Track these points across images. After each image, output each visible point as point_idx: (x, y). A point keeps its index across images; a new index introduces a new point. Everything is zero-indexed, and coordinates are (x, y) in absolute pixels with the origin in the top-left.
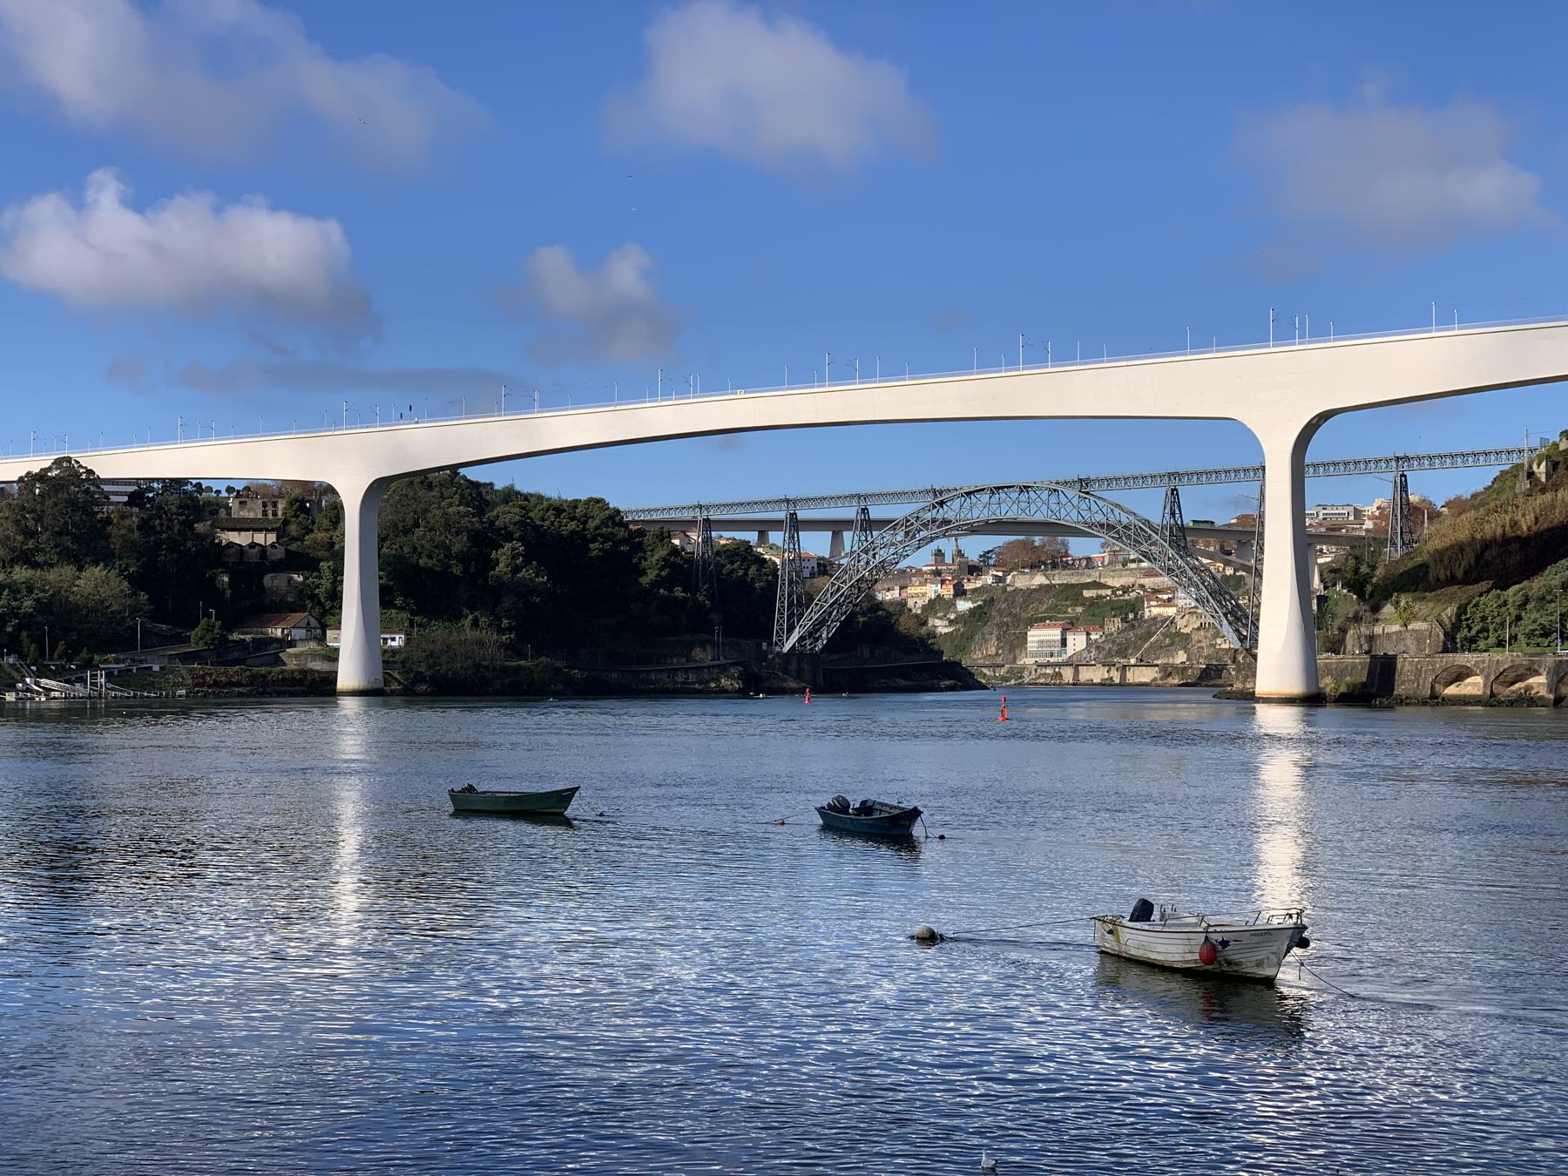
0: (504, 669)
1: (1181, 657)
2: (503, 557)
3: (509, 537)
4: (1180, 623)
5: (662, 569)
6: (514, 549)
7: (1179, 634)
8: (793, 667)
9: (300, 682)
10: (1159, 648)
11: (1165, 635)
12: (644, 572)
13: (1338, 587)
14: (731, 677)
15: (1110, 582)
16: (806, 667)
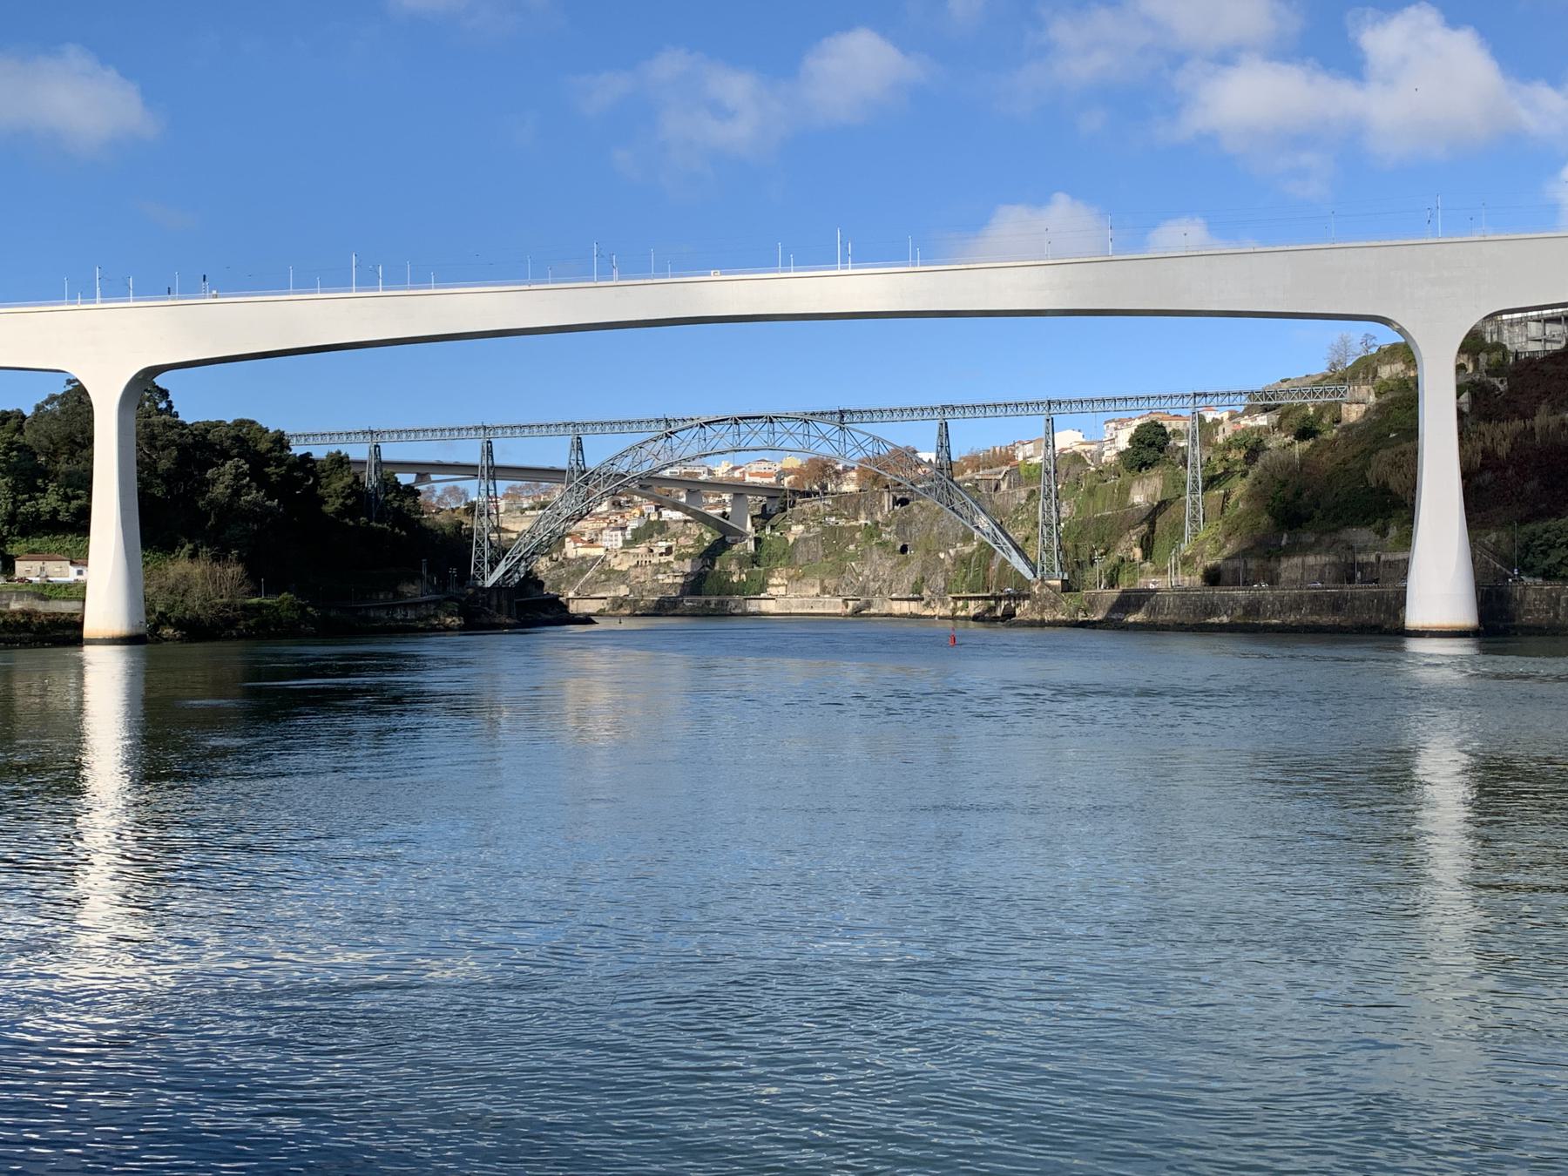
0: (245, 607)
1: (623, 591)
2: (223, 478)
3: (226, 455)
4: (614, 562)
5: (346, 498)
6: (238, 467)
7: (613, 571)
8: (494, 602)
9: (26, 627)
10: (593, 583)
11: (600, 572)
12: (322, 501)
13: (768, 531)
14: (450, 615)
15: (511, 527)
16: (504, 603)
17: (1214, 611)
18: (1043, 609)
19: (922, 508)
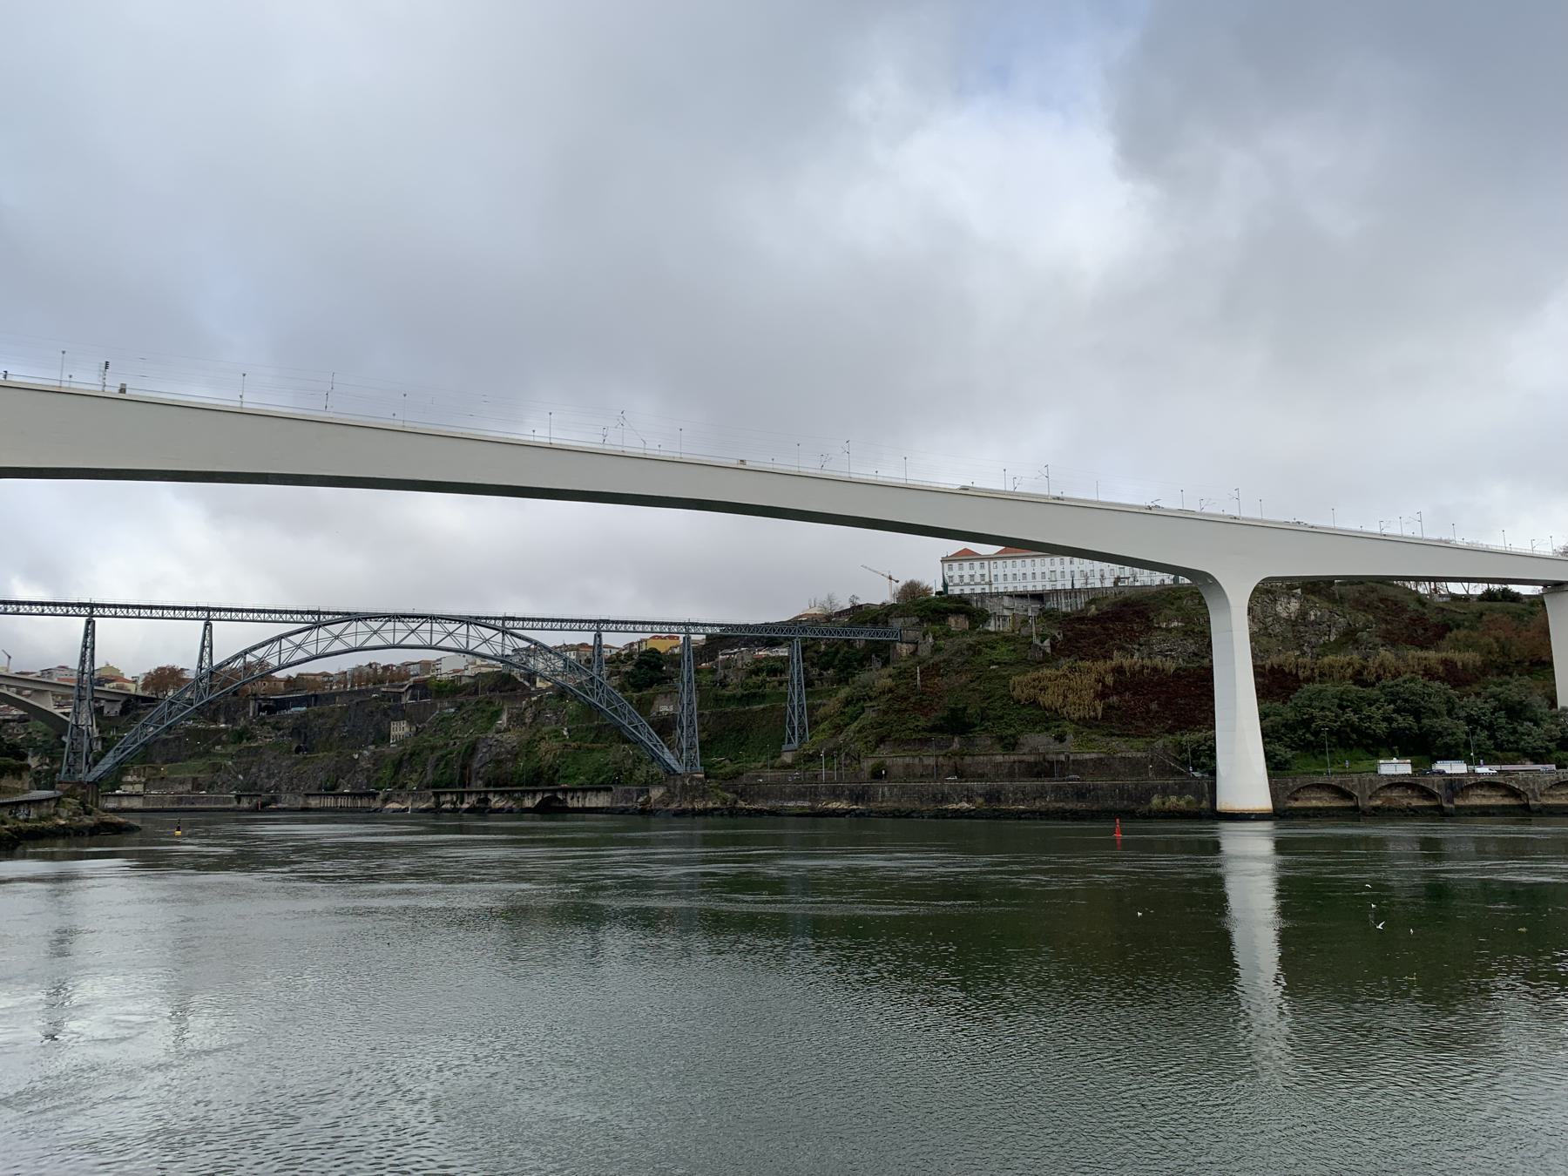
17: (945, 798)
18: (694, 798)
19: (320, 715)
